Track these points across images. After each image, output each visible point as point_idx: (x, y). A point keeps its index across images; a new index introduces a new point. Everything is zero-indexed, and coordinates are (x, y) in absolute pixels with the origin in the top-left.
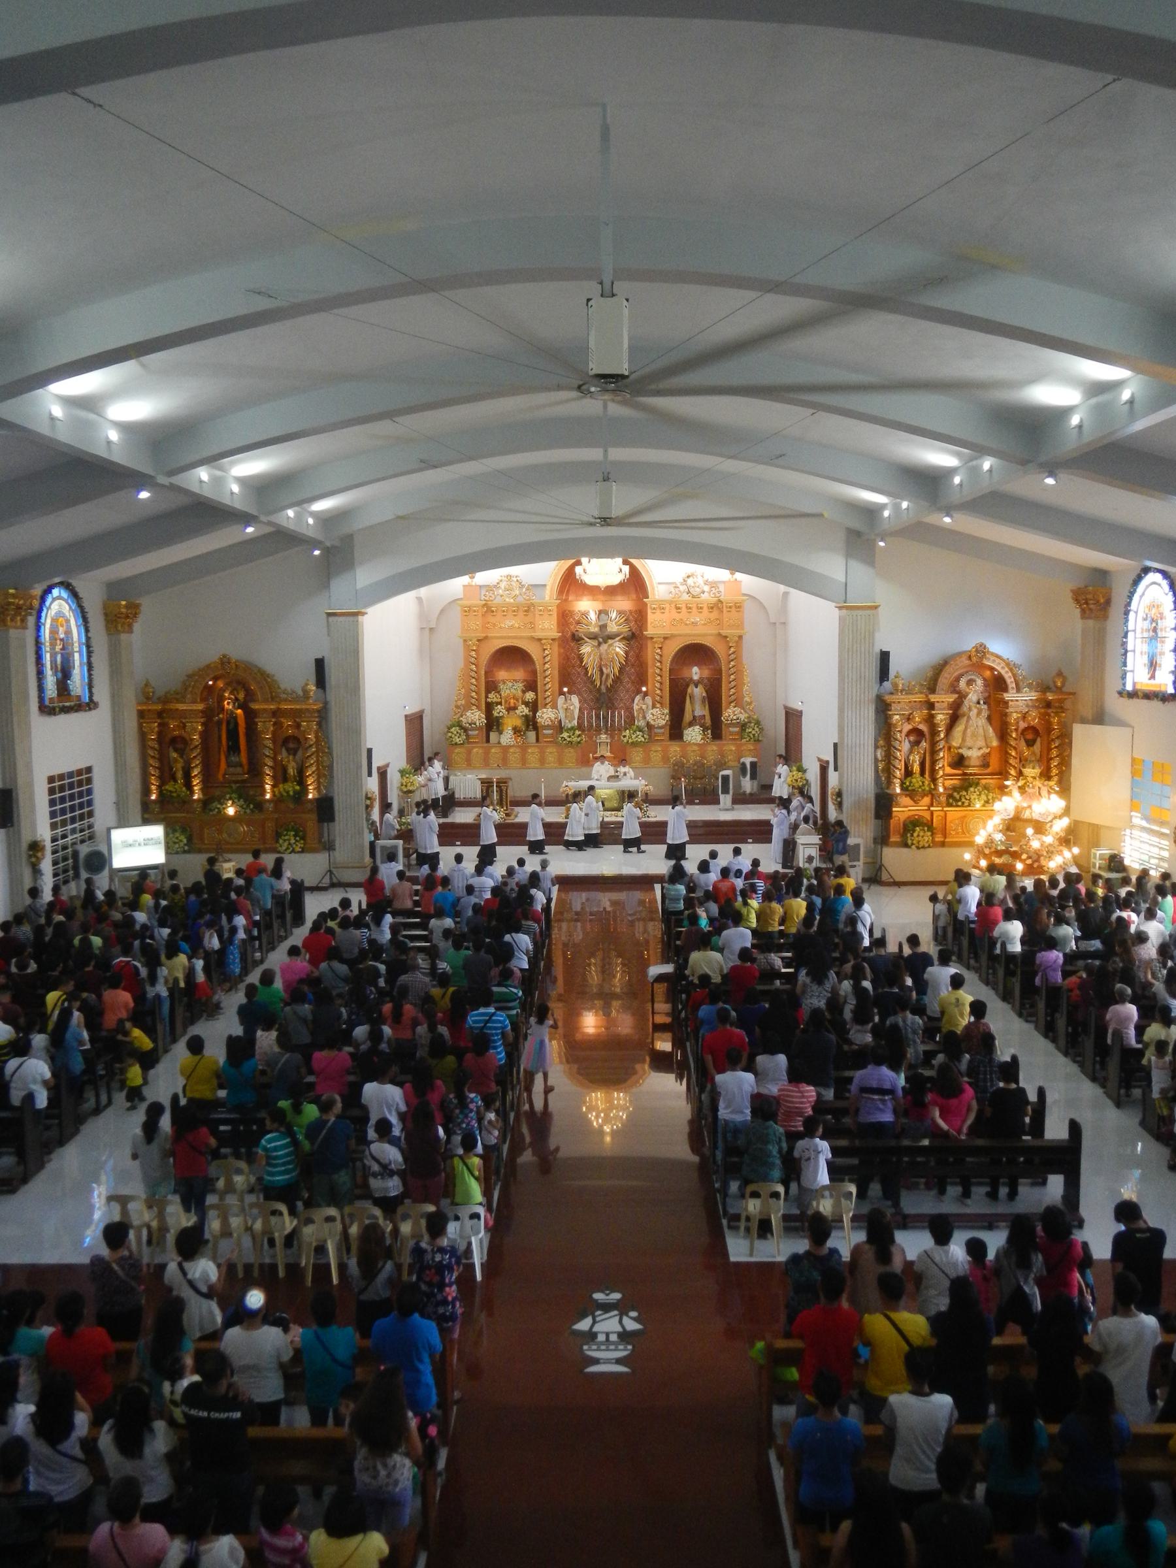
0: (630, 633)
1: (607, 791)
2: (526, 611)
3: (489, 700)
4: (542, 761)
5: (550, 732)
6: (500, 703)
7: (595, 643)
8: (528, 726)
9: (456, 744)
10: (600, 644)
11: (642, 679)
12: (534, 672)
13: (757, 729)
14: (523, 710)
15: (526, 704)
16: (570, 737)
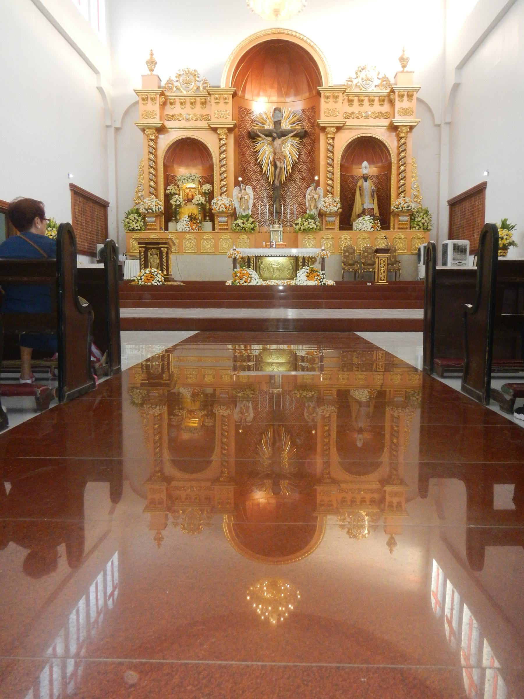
0: (303, 130)
1: (281, 260)
2: (202, 103)
3: (168, 192)
4: (216, 246)
5: (225, 219)
6: (179, 195)
7: (270, 139)
8: (205, 217)
9: (133, 230)
10: (274, 139)
11: (313, 170)
12: (211, 168)
13: (427, 219)
14: (199, 199)
15: (204, 194)
16: (243, 223)
